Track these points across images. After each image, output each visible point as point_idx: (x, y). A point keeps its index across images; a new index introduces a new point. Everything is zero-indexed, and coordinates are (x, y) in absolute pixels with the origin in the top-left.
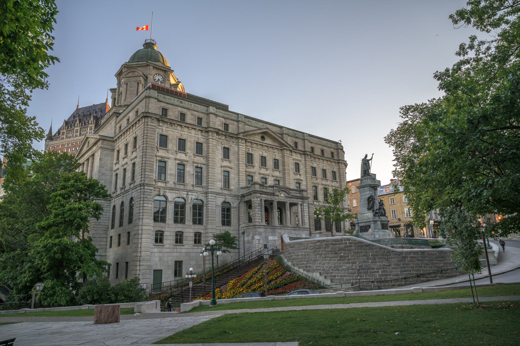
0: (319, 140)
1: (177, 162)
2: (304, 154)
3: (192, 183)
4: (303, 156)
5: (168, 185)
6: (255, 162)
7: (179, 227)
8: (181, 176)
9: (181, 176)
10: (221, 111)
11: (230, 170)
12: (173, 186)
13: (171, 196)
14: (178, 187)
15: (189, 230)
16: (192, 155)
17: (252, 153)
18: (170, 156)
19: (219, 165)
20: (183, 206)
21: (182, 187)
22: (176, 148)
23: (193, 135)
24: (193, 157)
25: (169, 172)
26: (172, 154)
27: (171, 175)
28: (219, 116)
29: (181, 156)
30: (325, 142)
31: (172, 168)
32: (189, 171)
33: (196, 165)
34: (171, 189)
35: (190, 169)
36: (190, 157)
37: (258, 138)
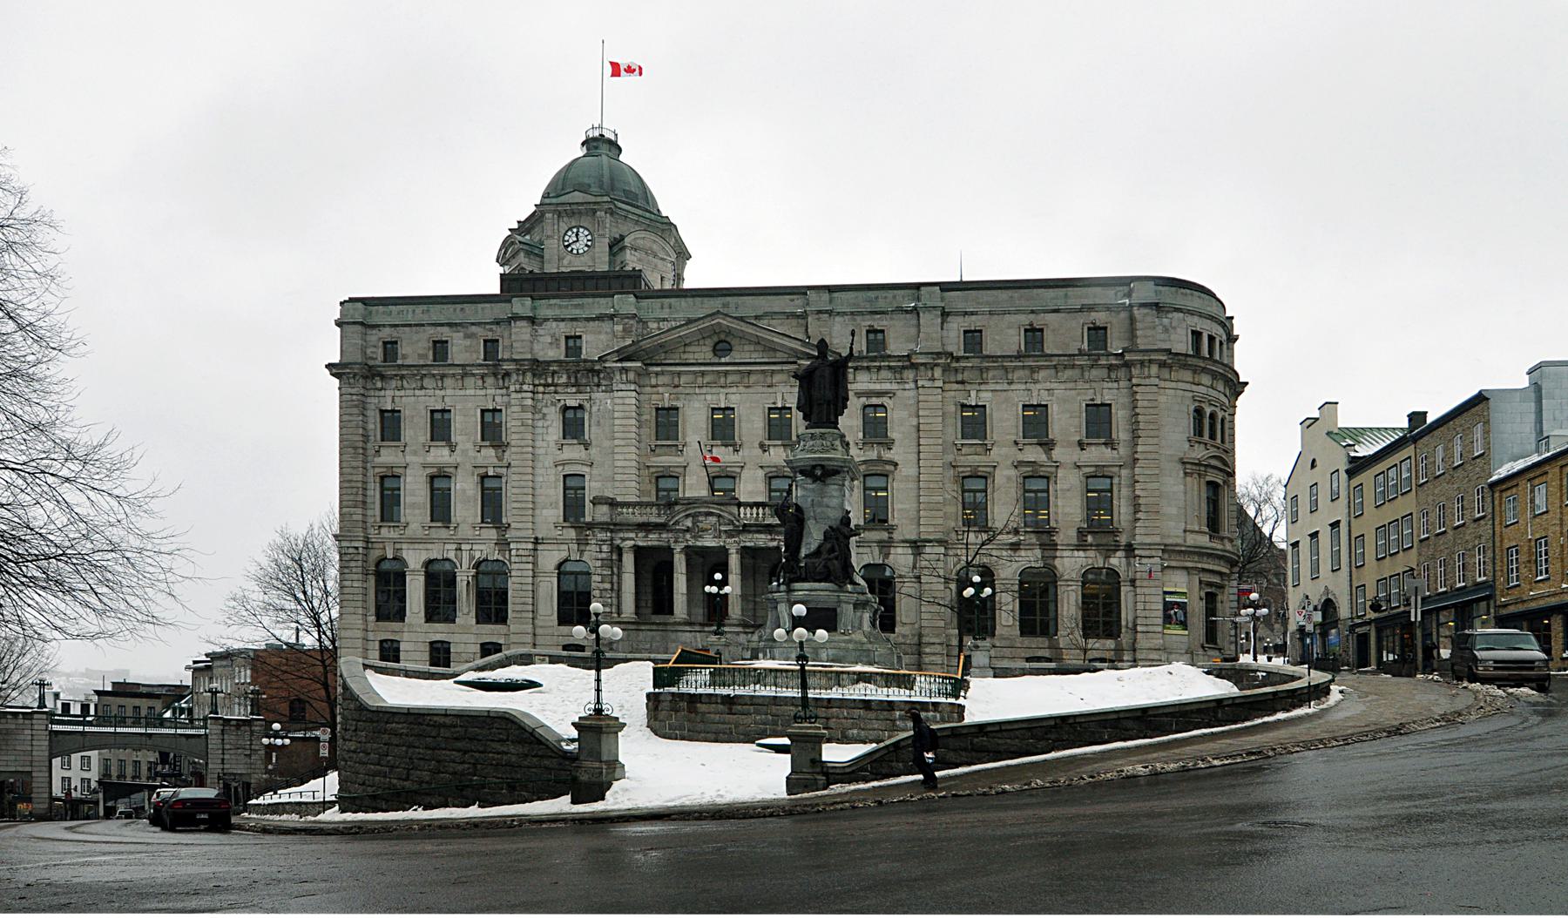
0: (1016, 294)
1: (429, 471)
2: (914, 366)
3: (470, 520)
4: (909, 374)
5: (409, 532)
6: (689, 431)
7: (439, 632)
8: (440, 508)
9: (440, 508)
10: (553, 301)
11: (587, 469)
12: (420, 533)
13: (414, 559)
14: (434, 534)
15: (465, 632)
16: (469, 446)
17: (679, 404)
18: (408, 459)
19: (549, 461)
20: (451, 581)
21: (444, 533)
22: (424, 436)
23: (472, 392)
24: (472, 453)
25: (407, 498)
26: (415, 453)
27: (413, 506)
28: (546, 320)
29: (440, 455)
30: (1051, 293)
31: (415, 492)
32: (464, 491)
33: (482, 471)
34: (413, 541)
35: (465, 489)
36: (464, 452)
37: (704, 353)
